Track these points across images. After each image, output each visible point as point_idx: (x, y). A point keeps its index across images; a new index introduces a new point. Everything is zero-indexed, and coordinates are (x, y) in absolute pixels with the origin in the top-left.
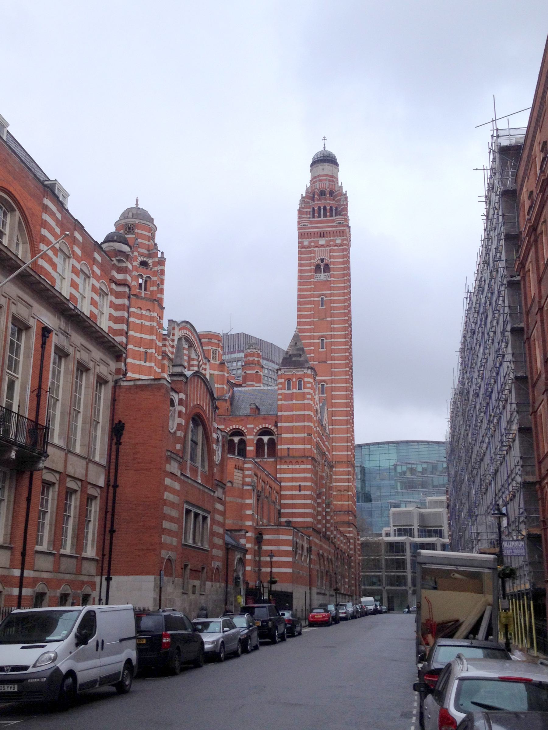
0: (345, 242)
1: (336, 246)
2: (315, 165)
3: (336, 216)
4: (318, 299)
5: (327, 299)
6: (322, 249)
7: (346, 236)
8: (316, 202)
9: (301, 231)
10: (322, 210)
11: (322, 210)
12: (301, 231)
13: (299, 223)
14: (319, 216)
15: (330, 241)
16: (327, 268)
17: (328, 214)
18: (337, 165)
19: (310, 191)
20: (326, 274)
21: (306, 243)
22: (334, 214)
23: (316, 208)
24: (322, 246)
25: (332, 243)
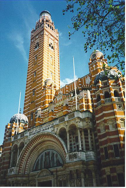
24: (37, 38)
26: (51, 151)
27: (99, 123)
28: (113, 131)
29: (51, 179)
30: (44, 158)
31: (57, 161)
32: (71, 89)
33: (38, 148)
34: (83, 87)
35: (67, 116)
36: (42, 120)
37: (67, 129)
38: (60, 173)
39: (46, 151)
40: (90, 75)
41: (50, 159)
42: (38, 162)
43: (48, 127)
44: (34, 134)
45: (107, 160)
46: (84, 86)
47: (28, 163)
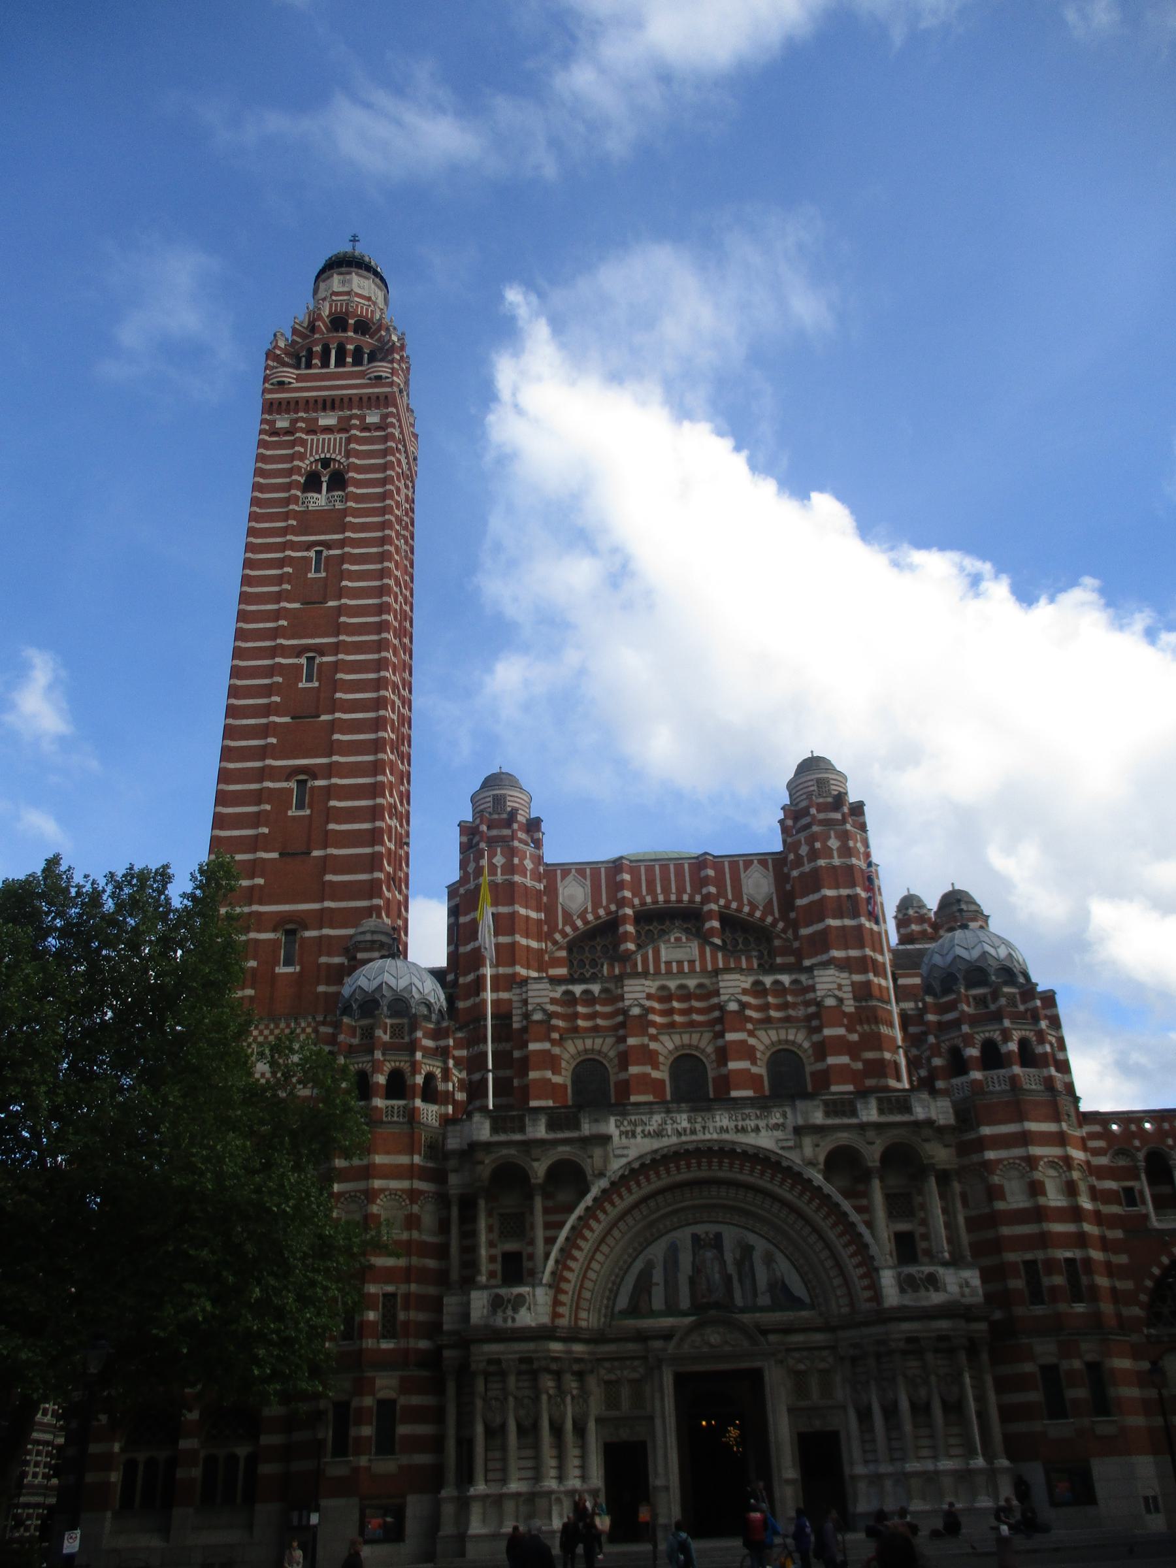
0: (390, 420)
1: (366, 428)
3: (371, 360)
4: (305, 554)
5: (332, 552)
6: (326, 437)
7: (396, 406)
8: (317, 336)
9: (268, 396)
12: (268, 396)
13: (266, 379)
14: (325, 364)
15: (351, 417)
16: (338, 481)
17: (349, 360)
18: (382, 280)
19: (305, 325)
20: (336, 493)
21: (283, 423)
23: (318, 349)
24: (328, 429)
25: (355, 422)
26: (730, 1235)
27: (999, 1161)
28: (1059, 1204)
29: (758, 1364)
30: (686, 1260)
32: (651, 890)
34: (727, 906)
36: (555, 1036)
38: (798, 1338)
39: (699, 1229)
40: (777, 864)
41: (731, 1269)
43: (751, 1123)
44: (659, 1134)
46: (734, 905)
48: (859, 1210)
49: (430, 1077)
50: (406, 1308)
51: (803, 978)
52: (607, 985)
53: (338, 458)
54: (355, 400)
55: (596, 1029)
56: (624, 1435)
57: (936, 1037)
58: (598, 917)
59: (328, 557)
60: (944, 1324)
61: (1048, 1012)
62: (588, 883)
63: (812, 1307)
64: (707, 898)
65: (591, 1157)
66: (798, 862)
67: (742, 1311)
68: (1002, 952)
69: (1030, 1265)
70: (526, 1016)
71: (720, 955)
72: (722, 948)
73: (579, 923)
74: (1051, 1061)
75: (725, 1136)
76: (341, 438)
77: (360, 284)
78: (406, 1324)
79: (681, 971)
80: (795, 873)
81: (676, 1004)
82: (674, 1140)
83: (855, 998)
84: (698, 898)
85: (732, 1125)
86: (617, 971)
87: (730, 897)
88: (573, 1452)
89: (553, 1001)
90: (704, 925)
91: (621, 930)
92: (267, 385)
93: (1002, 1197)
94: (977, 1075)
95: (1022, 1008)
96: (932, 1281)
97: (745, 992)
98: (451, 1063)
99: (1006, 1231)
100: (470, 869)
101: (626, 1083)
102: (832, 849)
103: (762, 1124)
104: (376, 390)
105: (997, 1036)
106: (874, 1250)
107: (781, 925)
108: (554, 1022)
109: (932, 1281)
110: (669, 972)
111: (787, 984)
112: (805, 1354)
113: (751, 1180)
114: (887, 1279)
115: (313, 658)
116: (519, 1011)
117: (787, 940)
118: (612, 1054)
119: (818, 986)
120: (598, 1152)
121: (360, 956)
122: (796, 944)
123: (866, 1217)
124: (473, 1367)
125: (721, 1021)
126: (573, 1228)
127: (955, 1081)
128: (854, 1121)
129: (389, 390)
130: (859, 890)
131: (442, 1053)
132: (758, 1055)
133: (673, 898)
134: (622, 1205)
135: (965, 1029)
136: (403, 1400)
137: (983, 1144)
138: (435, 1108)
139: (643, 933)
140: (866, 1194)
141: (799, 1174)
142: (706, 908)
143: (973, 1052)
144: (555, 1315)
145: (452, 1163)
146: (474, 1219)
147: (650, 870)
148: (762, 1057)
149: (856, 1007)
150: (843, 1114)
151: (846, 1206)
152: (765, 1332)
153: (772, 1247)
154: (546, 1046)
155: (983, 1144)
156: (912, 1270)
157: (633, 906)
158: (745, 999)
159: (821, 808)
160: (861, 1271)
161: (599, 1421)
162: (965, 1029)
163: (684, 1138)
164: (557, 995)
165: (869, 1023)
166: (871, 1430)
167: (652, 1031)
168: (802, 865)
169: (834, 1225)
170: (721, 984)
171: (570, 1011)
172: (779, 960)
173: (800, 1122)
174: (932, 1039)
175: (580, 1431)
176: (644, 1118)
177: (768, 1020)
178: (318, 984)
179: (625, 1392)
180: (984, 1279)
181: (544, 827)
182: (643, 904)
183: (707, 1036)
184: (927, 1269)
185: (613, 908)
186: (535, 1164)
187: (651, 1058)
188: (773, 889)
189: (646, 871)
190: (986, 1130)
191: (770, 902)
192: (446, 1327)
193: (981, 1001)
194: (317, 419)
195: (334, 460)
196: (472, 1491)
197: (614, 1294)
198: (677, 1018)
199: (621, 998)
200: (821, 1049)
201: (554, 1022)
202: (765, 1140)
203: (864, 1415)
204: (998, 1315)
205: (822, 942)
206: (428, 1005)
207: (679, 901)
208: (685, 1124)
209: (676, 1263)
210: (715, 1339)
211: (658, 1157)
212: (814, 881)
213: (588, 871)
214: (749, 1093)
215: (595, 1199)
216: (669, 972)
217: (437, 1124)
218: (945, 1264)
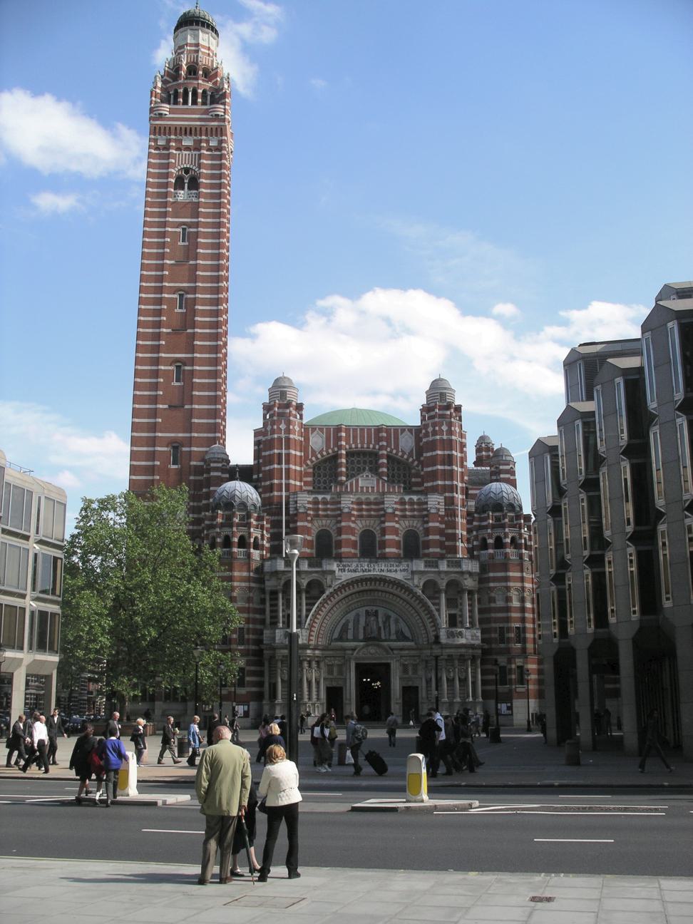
2: (181, 29)
3: (210, 104)
5: (192, 230)
6: (187, 153)
8: (181, 81)
10: (190, 93)
11: (190, 93)
13: (151, 110)
14: (185, 102)
16: (194, 184)
17: (200, 100)
22: (208, 102)
24: (188, 148)
26: (381, 612)
27: (496, 587)
29: (389, 661)
31: (397, 632)
32: (355, 442)
33: (352, 599)
34: (391, 452)
35: (445, 562)
36: (309, 518)
37: (443, 584)
38: (407, 652)
39: (369, 608)
40: (416, 431)
41: (381, 625)
42: (346, 625)
43: (395, 569)
45: (502, 646)
46: (394, 451)
47: (324, 625)
48: (434, 604)
49: (256, 538)
50: (248, 634)
51: (422, 497)
52: (334, 496)
53: (194, 168)
54: (204, 129)
55: (327, 516)
56: (334, 684)
57: (477, 532)
58: (328, 454)
59: (189, 232)
60: (463, 650)
61: (527, 523)
62: (324, 436)
63: (413, 641)
64: (381, 448)
65: (326, 579)
66: (427, 435)
67: (386, 640)
68: (511, 496)
69: (501, 629)
70: (296, 509)
71: (386, 484)
72: (388, 481)
73: (319, 456)
74: (523, 547)
75: (383, 574)
76: (195, 155)
77: (204, 38)
78: (248, 640)
79: (367, 491)
80: (424, 440)
81: (364, 507)
82: (361, 574)
83: (445, 506)
84: (377, 447)
85: (386, 569)
86: (338, 490)
87: (393, 447)
88: (314, 689)
89: (309, 502)
90: (379, 460)
91: (339, 461)
92: (152, 115)
93: (495, 602)
94: (491, 551)
95: (515, 522)
96: (460, 634)
97: (396, 503)
98: (265, 532)
99: (493, 615)
100: (269, 428)
101: (340, 541)
102: (443, 431)
103: (398, 569)
104: (216, 123)
105: (502, 536)
106: (439, 621)
107: (416, 463)
108: (309, 512)
109: (460, 634)
110: (362, 491)
111: (415, 500)
112: (408, 658)
113: (391, 590)
114: (443, 634)
115: (183, 295)
116: (293, 506)
117: (419, 470)
118: (334, 528)
119: (429, 503)
120: (329, 577)
121: (212, 465)
122: (422, 473)
123: (437, 607)
124: (277, 658)
125: (383, 516)
126: (318, 607)
127: (482, 552)
128: (436, 570)
129: (222, 124)
130: (454, 452)
131: (262, 527)
132: (400, 532)
133: (365, 446)
134: (337, 598)
135: (489, 531)
136: (248, 668)
137: (489, 580)
138: (258, 552)
139: (350, 461)
140: (439, 598)
141: (412, 590)
142: (381, 452)
143: (490, 541)
144: (309, 640)
145: (267, 577)
146: (277, 599)
147: (355, 430)
148: (401, 533)
149: (445, 509)
150: (433, 567)
151: (430, 603)
152: (392, 650)
153: (398, 617)
154: (306, 524)
155: (489, 580)
156: (453, 630)
157: (346, 449)
158: (395, 506)
159: (441, 408)
160: (434, 628)
161: (324, 679)
162: (489, 531)
163: (365, 573)
164: (310, 500)
165: (451, 516)
166: (431, 687)
167: (353, 519)
168: (428, 436)
169: (424, 611)
170: (385, 499)
171: (316, 506)
172: (413, 480)
173: (414, 569)
174: (475, 533)
175: (318, 683)
176: (349, 564)
177: (404, 516)
178: (190, 475)
179: (335, 669)
180: (482, 633)
181: (304, 407)
182: (350, 448)
183: (377, 522)
184: (459, 630)
185: (336, 449)
186: (303, 581)
187: (351, 531)
188: (414, 444)
189: (353, 431)
190: (491, 575)
191: (412, 451)
192: (264, 642)
193: (498, 519)
194: (181, 141)
195: (192, 169)
196: (276, 702)
197: (332, 632)
198: (364, 513)
199: (340, 503)
200: (427, 532)
201: (309, 512)
202: (399, 576)
203: (428, 682)
204: (486, 646)
205: (433, 476)
206: (254, 505)
207: (368, 447)
208: (366, 567)
209: (358, 621)
210: (372, 651)
211: (354, 580)
212: (432, 446)
213: (325, 430)
214: (394, 550)
215: (327, 596)
216: (362, 491)
217: (258, 559)
218: (468, 628)
